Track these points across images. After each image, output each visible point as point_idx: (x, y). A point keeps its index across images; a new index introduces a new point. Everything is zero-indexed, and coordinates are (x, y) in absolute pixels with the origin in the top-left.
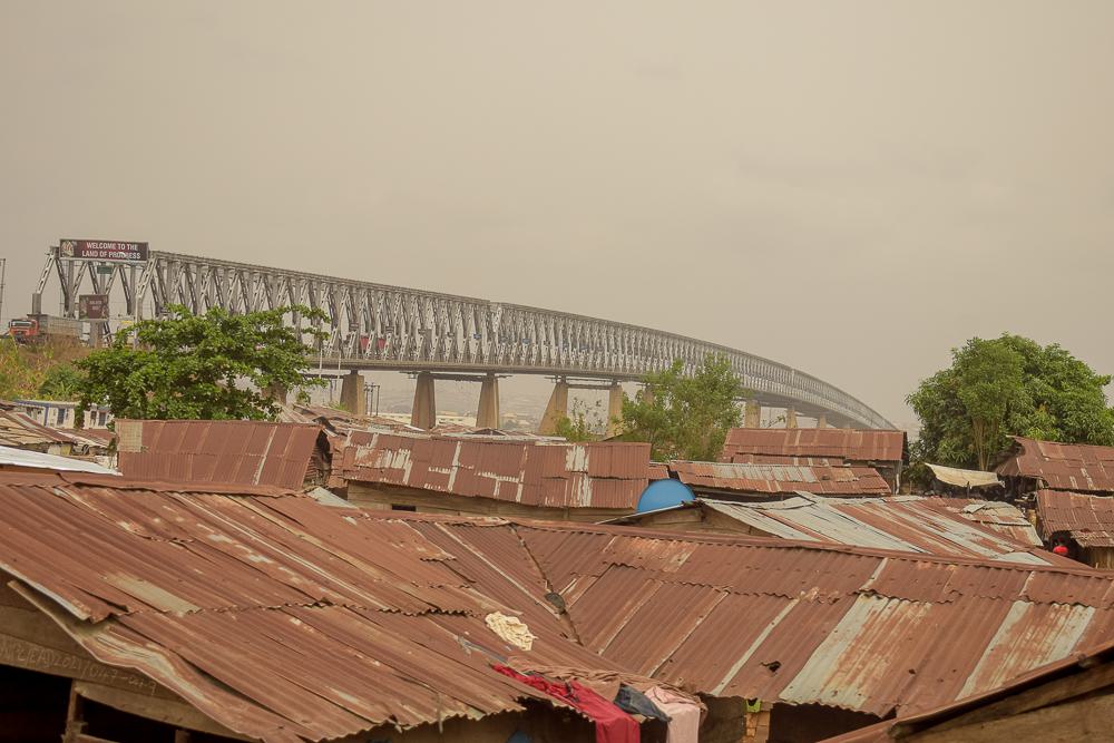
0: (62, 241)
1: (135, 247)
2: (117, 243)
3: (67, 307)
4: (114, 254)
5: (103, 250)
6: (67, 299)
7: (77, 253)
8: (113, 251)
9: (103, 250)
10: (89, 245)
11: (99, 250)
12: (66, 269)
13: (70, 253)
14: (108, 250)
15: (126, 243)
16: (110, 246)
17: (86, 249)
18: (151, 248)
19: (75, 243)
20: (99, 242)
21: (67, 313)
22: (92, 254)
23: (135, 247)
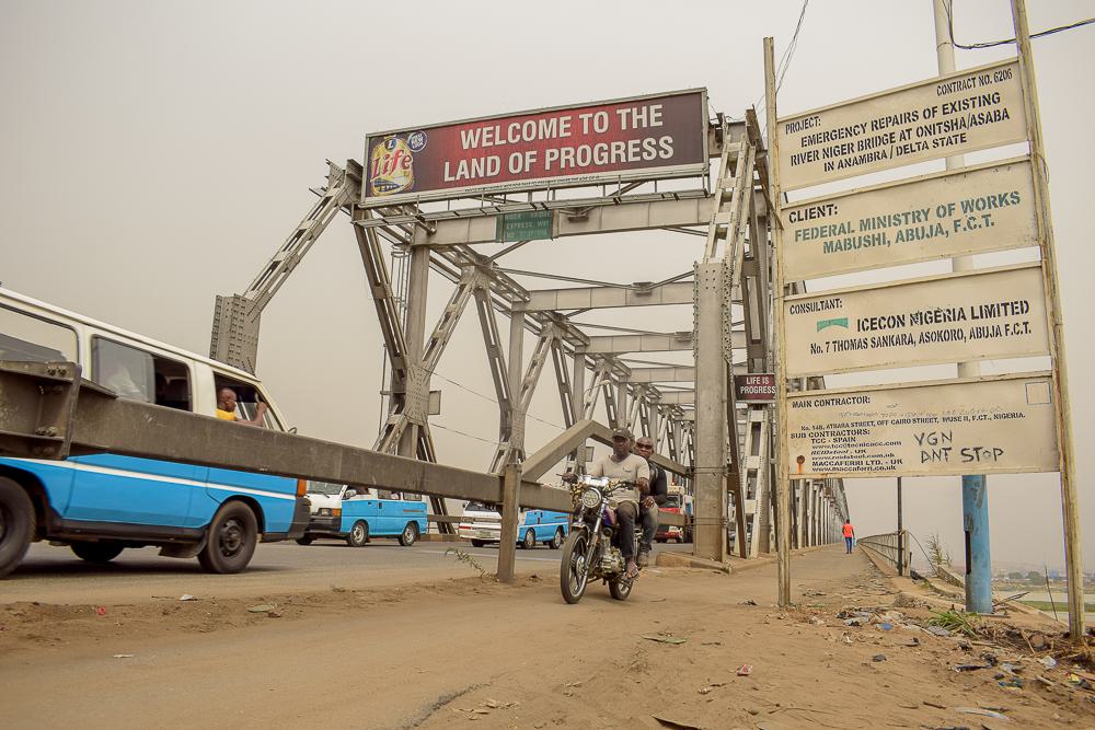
0: (374, 141)
1: (652, 116)
3: (399, 399)
4: (566, 155)
5: (522, 147)
6: (400, 374)
7: (427, 174)
8: (559, 143)
9: (522, 147)
10: (468, 140)
11: (504, 152)
12: (397, 286)
13: (401, 177)
14: (540, 146)
16: (545, 129)
17: (459, 155)
19: (418, 140)
21: (397, 419)
22: (479, 167)
23: (652, 116)
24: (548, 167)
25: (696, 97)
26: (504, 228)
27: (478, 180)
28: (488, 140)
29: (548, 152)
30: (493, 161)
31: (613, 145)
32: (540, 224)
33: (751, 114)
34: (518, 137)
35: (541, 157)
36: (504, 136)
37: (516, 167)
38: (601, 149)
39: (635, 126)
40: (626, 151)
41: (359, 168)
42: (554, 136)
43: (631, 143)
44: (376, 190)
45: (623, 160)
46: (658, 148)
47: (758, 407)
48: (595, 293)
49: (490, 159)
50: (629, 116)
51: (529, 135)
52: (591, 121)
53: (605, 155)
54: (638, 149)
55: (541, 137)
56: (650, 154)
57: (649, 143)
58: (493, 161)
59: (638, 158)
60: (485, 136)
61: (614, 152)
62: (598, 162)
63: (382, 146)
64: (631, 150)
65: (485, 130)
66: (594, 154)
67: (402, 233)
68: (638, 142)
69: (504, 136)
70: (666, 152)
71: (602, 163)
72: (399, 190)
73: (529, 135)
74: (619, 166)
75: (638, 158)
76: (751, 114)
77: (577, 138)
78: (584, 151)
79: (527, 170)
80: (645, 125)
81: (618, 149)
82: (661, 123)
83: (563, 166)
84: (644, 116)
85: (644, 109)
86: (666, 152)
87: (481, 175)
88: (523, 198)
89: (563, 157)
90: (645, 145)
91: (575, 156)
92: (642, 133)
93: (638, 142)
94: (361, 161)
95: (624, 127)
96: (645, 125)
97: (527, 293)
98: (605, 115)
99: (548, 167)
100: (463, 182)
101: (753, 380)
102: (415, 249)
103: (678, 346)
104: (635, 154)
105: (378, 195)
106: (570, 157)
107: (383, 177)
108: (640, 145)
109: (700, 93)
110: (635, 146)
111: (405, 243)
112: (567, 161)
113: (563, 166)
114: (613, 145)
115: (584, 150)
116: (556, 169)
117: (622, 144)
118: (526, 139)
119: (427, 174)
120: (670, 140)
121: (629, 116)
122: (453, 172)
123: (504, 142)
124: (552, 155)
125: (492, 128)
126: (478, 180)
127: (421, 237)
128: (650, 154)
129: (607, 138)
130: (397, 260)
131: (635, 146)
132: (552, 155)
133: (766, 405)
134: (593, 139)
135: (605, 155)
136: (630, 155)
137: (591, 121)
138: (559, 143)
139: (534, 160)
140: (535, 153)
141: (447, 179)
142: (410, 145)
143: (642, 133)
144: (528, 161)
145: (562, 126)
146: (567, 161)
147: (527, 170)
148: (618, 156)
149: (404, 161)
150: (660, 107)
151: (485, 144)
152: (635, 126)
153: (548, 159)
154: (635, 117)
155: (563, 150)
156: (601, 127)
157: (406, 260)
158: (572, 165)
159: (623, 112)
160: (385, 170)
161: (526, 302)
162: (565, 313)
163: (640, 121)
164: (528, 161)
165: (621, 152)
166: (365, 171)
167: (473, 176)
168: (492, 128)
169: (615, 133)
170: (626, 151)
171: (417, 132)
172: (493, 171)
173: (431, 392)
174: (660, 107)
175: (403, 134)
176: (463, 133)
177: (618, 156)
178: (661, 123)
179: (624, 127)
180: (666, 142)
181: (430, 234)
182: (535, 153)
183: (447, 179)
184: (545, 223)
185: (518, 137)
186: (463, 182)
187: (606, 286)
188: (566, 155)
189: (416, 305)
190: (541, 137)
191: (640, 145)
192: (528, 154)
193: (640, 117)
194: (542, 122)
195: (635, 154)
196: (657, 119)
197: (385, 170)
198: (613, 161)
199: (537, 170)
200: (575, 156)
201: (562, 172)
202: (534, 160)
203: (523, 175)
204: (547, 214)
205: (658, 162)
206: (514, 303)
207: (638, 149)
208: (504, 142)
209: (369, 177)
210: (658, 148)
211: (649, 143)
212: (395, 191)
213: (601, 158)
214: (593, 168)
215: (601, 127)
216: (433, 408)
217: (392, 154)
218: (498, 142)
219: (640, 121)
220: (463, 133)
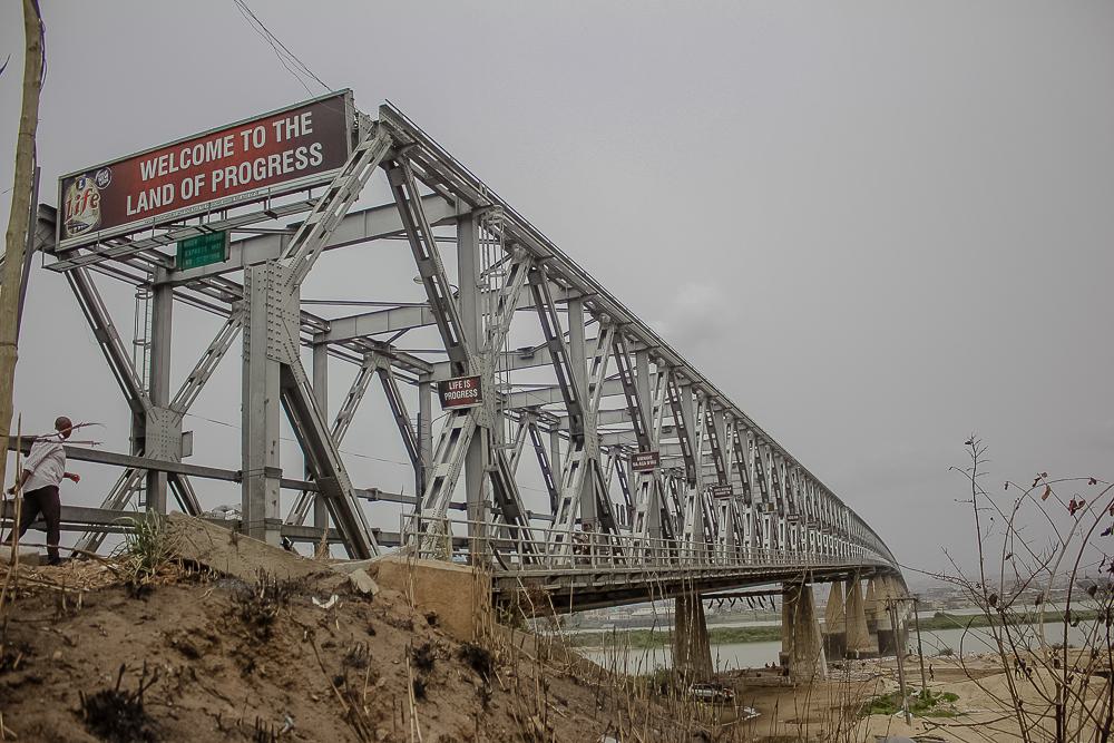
0: (66, 182)
1: (302, 125)
2: (234, 129)
4: (230, 175)
5: (192, 172)
8: (222, 163)
9: (192, 172)
10: (147, 171)
11: (176, 179)
13: (89, 217)
14: (207, 168)
15: (266, 120)
16: (213, 151)
18: (367, 106)
19: (103, 178)
20: (176, 147)
22: (157, 197)
23: (302, 125)
24: (214, 189)
25: (339, 100)
26: (183, 254)
27: (156, 210)
28: (164, 169)
29: (214, 173)
30: (168, 189)
31: (270, 158)
32: (214, 247)
33: (384, 109)
34: (189, 162)
35: (208, 180)
36: (176, 164)
37: (187, 194)
38: (260, 165)
39: (288, 137)
40: (281, 163)
41: (53, 211)
42: (219, 157)
43: (285, 154)
44: (69, 232)
45: (279, 173)
46: (309, 155)
47: (462, 412)
48: (392, 314)
49: (165, 187)
50: (283, 127)
51: (198, 159)
52: (251, 136)
53: (263, 169)
54: (291, 160)
55: (208, 160)
56: (302, 163)
57: (301, 152)
58: (168, 189)
59: (292, 169)
60: (161, 165)
61: (271, 166)
62: (257, 178)
63: (74, 187)
64: (286, 161)
65: (161, 159)
66: (254, 170)
67: (144, 275)
68: (292, 152)
69: (176, 164)
70: (316, 159)
71: (260, 178)
72: (88, 229)
73: (198, 159)
74: (277, 179)
75: (292, 169)
76: (384, 109)
77: (239, 156)
78: (245, 167)
79: (197, 194)
80: (297, 135)
81: (279, 162)
82: (311, 131)
83: (227, 186)
84: (296, 126)
85: (296, 118)
86: (316, 159)
87: (158, 205)
88: (195, 222)
89: (228, 177)
90: (298, 155)
91: (237, 175)
92: (295, 143)
93: (292, 152)
94: (55, 204)
95: (279, 140)
96: (297, 135)
97: (327, 323)
98: (262, 129)
99: (214, 189)
100: (144, 214)
101: (455, 385)
102: (157, 289)
103: (524, 363)
104: (289, 165)
105: (71, 237)
106: (234, 176)
107: (75, 218)
108: (293, 156)
109: (343, 95)
110: (289, 157)
111: (146, 284)
112: (231, 180)
113: (227, 186)
114: (270, 158)
115: (245, 167)
116: (222, 191)
117: (277, 156)
118: (196, 163)
119: (112, 210)
120: (320, 147)
121: (283, 127)
122: (134, 206)
123: (177, 169)
124: (218, 176)
125: (166, 156)
126: (156, 210)
127: (163, 277)
128: (302, 163)
129: (264, 152)
130: (142, 303)
131: (289, 157)
132: (218, 176)
133: (469, 409)
134: (253, 154)
135: (263, 169)
136: (285, 165)
137: (251, 136)
138: (222, 163)
139: (203, 184)
140: (203, 176)
141: (129, 212)
142: (97, 183)
143: (295, 143)
144: (198, 185)
145: (227, 146)
146: (231, 180)
147: (197, 194)
148: (274, 169)
149: (92, 200)
150: (310, 114)
151: (161, 173)
152: (288, 137)
153: (215, 181)
154: (289, 128)
155: (227, 169)
156: (259, 142)
157: (151, 301)
158: (235, 184)
159: (278, 124)
160: (77, 211)
161: (326, 332)
162: (384, 338)
163: (293, 131)
164: (198, 185)
165: (277, 165)
166: (59, 213)
167: (151, 207)
168: (166, 156)
169: (273, 147)
170: (281, 163)
171: (103, 168)
172: (168, 199)
173: (183, 434)
174: (310, 114)
175: (91, 173)
176: (142, 164)
177: (274, 169)
178: (311, 131)
179: (279, 140)
180: (316, 149)
181: (170, 272)
182: (203, 176)
183: (129, 212)
184: (218, 246)
185: (189, 162)
186: (144, 214)
187: (403, 307)
188: (230, 175)
189: (158, 348)
190: (208, 160)
191: (293, 156)
192: (197, 178)
193: (292, 127)
194: (209, 144)
195: (289, 165)
196: (308, 127)
197: (77, 211)
198: (270, 175)
199: (206, 194)
200: (237, 175)
201: (226, 192)
202: (203, 184)
203: (194, 200)
204: (219, 236)
205: (310, 170)
206: (316, 335)
207: (291, 160)
208: (177, 169)
209: (62, 221)
210: (309, 155)
211: (301, 152)
212: (86, 231)
213: (260, 173)
214: (254, 184)
215: (259, 142)
216: (185, 451)
217: (82, 194)
218: (172, 170)
219: (293, 131)
220: (142, 164)
